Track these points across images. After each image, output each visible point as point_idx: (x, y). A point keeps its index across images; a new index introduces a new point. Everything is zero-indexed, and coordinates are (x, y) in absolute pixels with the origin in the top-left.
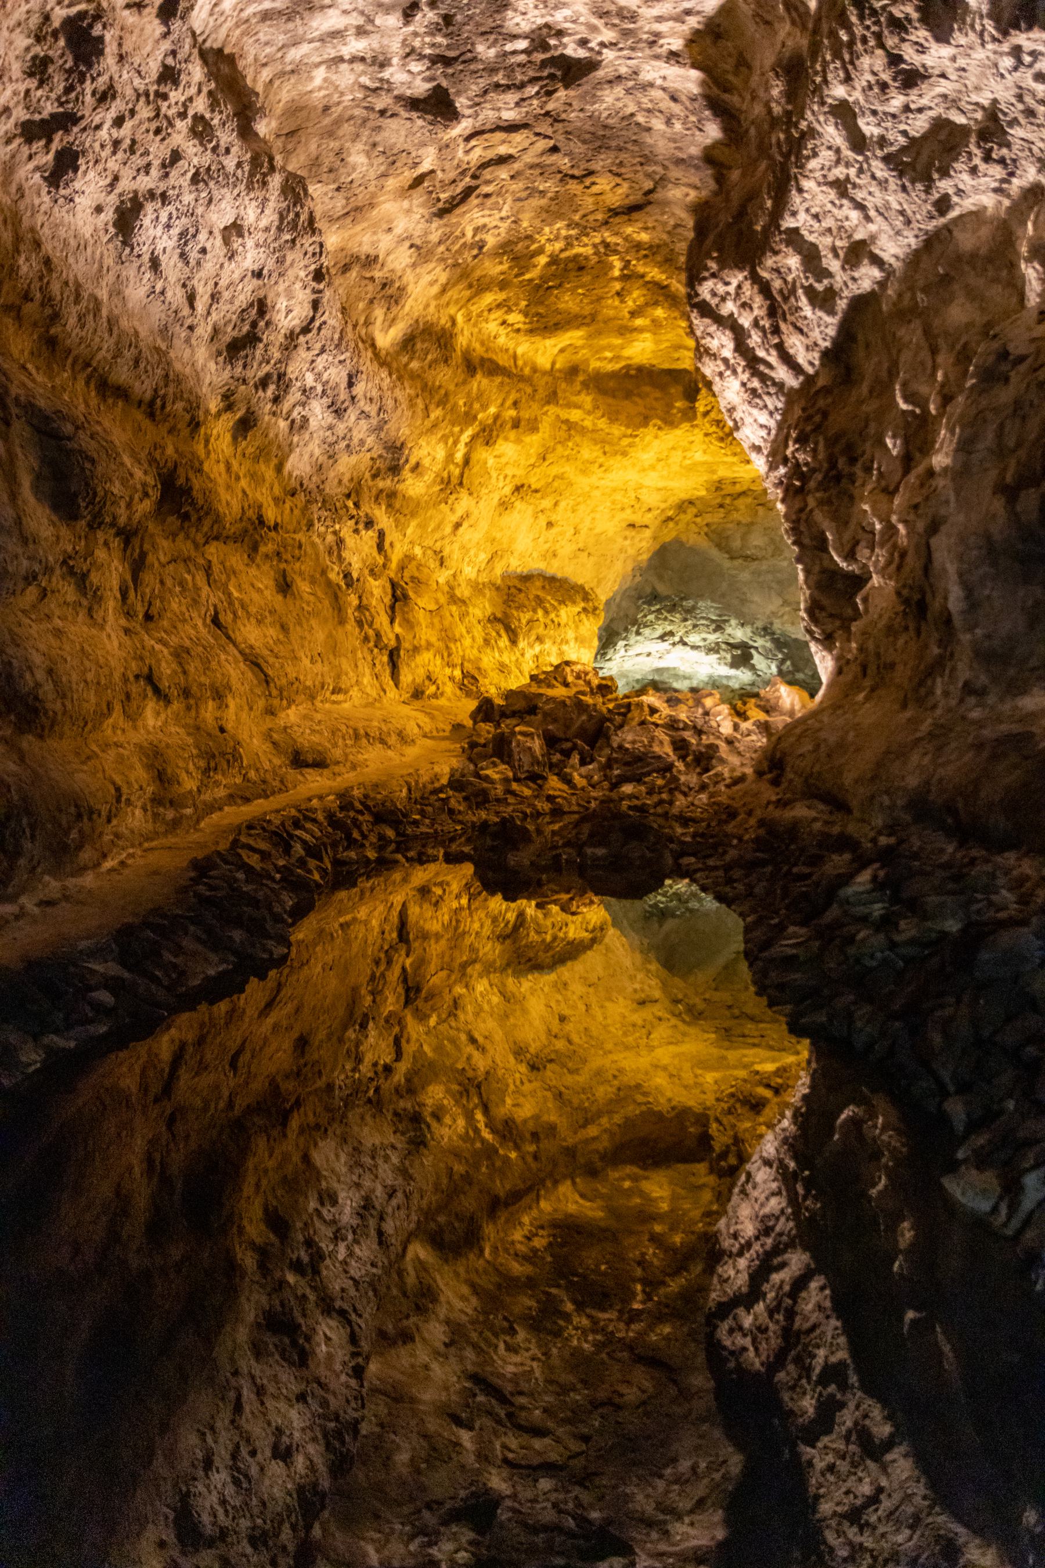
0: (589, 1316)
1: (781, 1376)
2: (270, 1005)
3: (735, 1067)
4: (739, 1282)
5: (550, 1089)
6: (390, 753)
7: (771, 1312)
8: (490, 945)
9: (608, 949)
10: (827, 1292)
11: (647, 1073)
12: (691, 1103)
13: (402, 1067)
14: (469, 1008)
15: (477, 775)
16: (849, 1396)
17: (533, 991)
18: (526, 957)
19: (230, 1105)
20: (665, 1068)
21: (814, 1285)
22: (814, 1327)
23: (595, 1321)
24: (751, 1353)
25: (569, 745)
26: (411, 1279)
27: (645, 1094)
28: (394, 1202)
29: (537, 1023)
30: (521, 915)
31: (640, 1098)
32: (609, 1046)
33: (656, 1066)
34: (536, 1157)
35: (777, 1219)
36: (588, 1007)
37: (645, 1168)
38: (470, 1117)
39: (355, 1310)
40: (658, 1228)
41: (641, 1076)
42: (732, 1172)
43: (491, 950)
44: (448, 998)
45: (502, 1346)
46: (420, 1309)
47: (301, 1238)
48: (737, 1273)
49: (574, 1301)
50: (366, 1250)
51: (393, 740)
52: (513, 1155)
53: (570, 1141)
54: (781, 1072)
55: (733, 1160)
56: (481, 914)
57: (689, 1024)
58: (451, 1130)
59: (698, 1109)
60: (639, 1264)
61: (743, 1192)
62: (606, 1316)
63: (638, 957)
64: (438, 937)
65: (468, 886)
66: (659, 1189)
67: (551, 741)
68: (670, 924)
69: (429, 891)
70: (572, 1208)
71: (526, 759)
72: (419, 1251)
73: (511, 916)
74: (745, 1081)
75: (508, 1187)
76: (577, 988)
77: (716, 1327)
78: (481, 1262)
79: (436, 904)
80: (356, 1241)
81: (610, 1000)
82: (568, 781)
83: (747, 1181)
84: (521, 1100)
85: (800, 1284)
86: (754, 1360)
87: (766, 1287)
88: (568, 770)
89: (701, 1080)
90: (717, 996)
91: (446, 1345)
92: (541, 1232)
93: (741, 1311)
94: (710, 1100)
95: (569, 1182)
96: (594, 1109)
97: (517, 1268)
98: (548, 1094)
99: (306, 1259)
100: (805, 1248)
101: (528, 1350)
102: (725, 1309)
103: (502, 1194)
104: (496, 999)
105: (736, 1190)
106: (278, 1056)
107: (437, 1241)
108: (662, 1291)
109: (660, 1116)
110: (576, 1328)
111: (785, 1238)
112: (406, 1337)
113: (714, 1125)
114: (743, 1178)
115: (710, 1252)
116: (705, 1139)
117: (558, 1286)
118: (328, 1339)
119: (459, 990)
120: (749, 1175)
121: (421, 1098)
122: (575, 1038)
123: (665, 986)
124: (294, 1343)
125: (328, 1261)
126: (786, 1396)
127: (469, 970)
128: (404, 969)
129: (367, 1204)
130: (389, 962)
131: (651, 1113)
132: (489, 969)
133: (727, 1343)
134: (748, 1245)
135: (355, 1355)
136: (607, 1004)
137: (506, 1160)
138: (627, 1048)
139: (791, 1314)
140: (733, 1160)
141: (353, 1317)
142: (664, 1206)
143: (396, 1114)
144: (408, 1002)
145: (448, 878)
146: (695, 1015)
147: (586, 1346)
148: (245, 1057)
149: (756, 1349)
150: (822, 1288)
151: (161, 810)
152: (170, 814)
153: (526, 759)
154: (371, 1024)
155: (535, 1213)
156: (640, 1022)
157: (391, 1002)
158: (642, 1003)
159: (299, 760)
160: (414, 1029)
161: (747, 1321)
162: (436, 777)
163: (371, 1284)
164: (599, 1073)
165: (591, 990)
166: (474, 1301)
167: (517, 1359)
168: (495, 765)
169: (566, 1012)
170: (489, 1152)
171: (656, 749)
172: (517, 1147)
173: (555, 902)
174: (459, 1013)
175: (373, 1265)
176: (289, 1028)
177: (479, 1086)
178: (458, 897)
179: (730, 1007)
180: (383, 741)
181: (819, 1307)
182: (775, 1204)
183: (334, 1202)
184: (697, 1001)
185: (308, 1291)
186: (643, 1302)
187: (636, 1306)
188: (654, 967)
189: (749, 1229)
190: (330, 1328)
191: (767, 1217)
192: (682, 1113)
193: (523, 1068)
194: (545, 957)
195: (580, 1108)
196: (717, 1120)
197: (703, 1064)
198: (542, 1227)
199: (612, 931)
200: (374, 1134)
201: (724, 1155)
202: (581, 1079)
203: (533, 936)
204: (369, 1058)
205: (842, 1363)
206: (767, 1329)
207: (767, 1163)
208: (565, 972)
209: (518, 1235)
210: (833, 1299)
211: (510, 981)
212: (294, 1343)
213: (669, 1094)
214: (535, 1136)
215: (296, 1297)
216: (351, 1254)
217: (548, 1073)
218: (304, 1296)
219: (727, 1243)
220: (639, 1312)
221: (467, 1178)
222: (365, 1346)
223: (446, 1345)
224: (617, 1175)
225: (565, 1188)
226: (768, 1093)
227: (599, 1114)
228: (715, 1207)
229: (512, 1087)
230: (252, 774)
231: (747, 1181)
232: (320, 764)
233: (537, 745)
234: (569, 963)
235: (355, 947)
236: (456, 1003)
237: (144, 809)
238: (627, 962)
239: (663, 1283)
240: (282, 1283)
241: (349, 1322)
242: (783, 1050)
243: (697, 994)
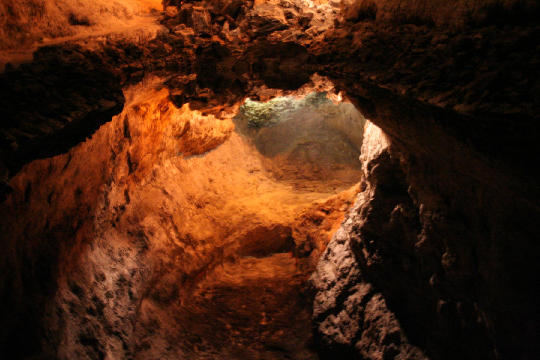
0: (239, 330)
1: (360, 343)
2: (66, 167)
3: (304, 203)
4: (330, 303)
5: (208, 218)
6: (120, 22)
7: (350, 315)
8: (171, 141)
9: (232, 143)
10: (383, 300)
11: (258, 208)
12: (282, 222)
13: (130, 208)
14: (162, 175)
15: (174, 33)
16: (402, 347)
17: (195, 167)
18: (192, 146)
19: (48, 224)
20: (267, 205)
21: (374, 298)
22: (378, 318)
23: (243, 332)
24: (341, 336)
25: (221, 18)
26: (145, 317)
27: (257, 219)
28: (135, 277)
29: (198, 183)
30: (188, 123)
31: (255, 221)
32: (237, 194)
33: (262, 204)
34: (204, 253)
35: (350, 269)
36: (224, 174)
37: (258, 257)
38: (168, 233)
39: (124, 332)
40: (270, 285)
41: (254, 210)
42: (308, 254)
43: (172, 143)
44: (151, 169)
45: (196, 348)
46: (152, 332)
47: (90, 297)
48: (328, 298)
49: (231, 324)
50: (125, 301)
51: (121, 13)
52: (192, 252)
53: (220, 245)
54: (329, 202)
55: (307, 249)
56: (167, 122)
57: (276, 182)
58: (159, 240)
59: (286, 225)
60: (263, 303)
61: (326, 259)
62: (249, 329)
63: (248, 148)
64: (146, 135)
65: (160, 106)
66: (266, 268)
67: (213, 16)
68: (262, 131)
69: (139, 109)
70: (223, 279)
71: (201, 25)
72: (147, 304)
73: (183, 124)
74: (310, 209)
75: (191, 268)
76: (217, 165)
77: (319, 325)
78: (180, 308)
79: (143, 116)
80: (118, 298)
81: (235, 170)
82: (223, 37)
83: (328, 253)
84: (194, 224)
85: (366, 299)
86: (343, 338)
87: (346, 303)
88: (223, 32)
89: (286, 210)
90: (289, 167)
91: (168, 349)
92: (209, 291)
93: (332, 317)
94: (292, 219)
95: (220, 266)
96: (231, 227)
97: (198, 310)
98: (208, 220)
99: (95, 308)
100: (366, 282)
101: (209, 349)
102: (323, 316)
103: (188, 272)
104: (175, 171)
105: (322, 258)
106: (67, 199)
107: (157, 298)
108: (276, 314)
109: (265, 230)
110: (234, 337)
111: (355, 278)
112: (147, 346)
113: (295, 233)
114: (326, 252)
115: (307, 293)
116: (291, 239)
117: (221, 317)
118: (112, 347)
119: (156, 166)
120: (329, 250)
121: (142, 223)
122: (219, 192)
123: (263, 162)
124: (96, 350)
125: (106, 309)
126: (364, 353)
127: (160, 155)
128: (128, 154)
129: (122, 280)
130: (121, 149)
131: (261, 228)
132: (171, 154)
133: (326, 332)
134: (333, 284)
135: (127, 354)
136: (234, 173)
137: (189, 255)
138: (246, 195)
139: (362, 314)
140: (307, 249)
141: (123, 336)
142: (271, 275)
143: (129, 233)
144: (131, 171)
145: (149, 101)
146: (279, 178)
147: (240, 345)
148: (54, 197)
149: (343, 333)
150: (380, 299)
151: (13, 32)
152: (19, 36)
153: (201, 25)
154: (113, 184)
155: (204, 282)
156: (252, 182)
157: (122, 172)
158: (252, 172)
159: (74, 20)
160: (134, 187)
161: (337, 321)
162: (150, 35)
163: (130, 319)
164: (233, 208)
165: (225, 165)
166: (178, 326)
167: (205, 353)
168: (183, 28)
169: (213, 177)
170: (180, 251)
171: (277, 18)
172: (194, 248)
173: (212, 113)
174: (157, 178)
175: (130, 309)
176: (73, 183)
177: (171, 217)
178: (155, 112)
179: (296, 173)
180: (116, 15)
181: (380, 308)
182: (348, 262)
183: (103, 278)
184: (279, 170)
185: (98, 323)
186: (267, 321)
187: (263, 323)
188: (256, 152)
189: (332, 276)
190: (113, 342)
191: (346, 268)
192: (278, 227)
193: (193, 207)
194: (200, 148)
195: (224, 227)
196: (296, 230)
197: (286, 202)
198: (209, 289)
199: (233, 134)
200: (118, 243)
201: (302, 246)
202: (225, 211)
203: (195, 136)
204: (113, 203)
205: (396, 333)
206: (349, 323)
207: (342, 242)
208: (210, 156)
209: (196, 294)
210: (387, 302)
211: (183, 162)
212: (96, 350)
213: (270, 218)
214: (203, 242)
215: (94, 327)
216: (117, 304)
217: (206, 209)
218: (98, 326)
219: (320, 285)
220: (265, 327)
221: (170, 265)
222: (132, 350)
223: (168, 349)
224: (244, 261)
225: (218, 269)
226: (323, 214)
227: (234, 230)
228: (299, 273)
229: (188, 218)
230: (52, 23)
231: (328, 253)
232: (86, 23)
233: (206, 17)
234: (212, 151)
235: (104, 138)
236: (155, 173)
237: (5, 31)
238: (242, 150)
239: (276, 311)
240: (85, 321)
241: (122, 339)
242: (327, 193)
243: (279, 166)
